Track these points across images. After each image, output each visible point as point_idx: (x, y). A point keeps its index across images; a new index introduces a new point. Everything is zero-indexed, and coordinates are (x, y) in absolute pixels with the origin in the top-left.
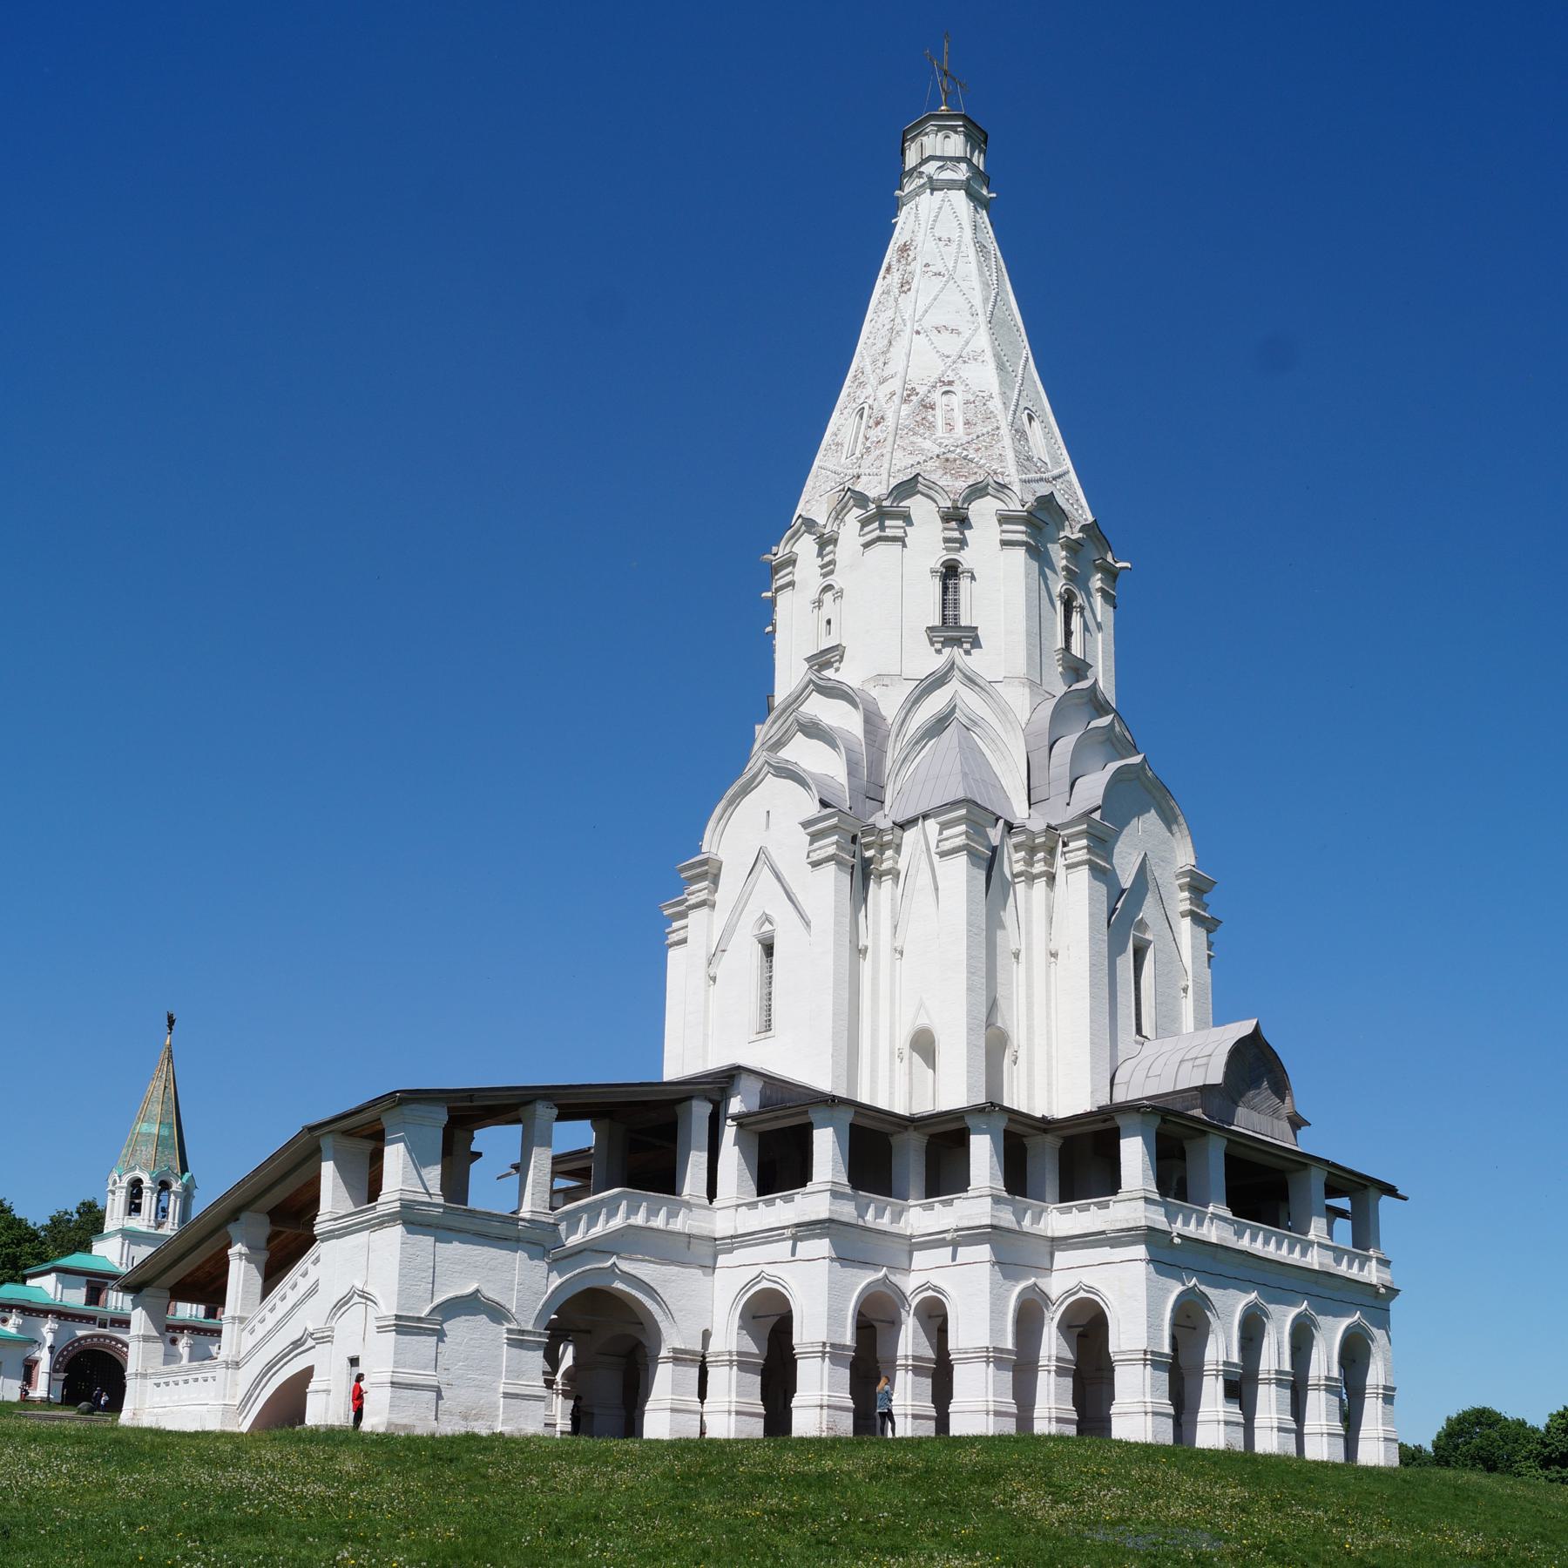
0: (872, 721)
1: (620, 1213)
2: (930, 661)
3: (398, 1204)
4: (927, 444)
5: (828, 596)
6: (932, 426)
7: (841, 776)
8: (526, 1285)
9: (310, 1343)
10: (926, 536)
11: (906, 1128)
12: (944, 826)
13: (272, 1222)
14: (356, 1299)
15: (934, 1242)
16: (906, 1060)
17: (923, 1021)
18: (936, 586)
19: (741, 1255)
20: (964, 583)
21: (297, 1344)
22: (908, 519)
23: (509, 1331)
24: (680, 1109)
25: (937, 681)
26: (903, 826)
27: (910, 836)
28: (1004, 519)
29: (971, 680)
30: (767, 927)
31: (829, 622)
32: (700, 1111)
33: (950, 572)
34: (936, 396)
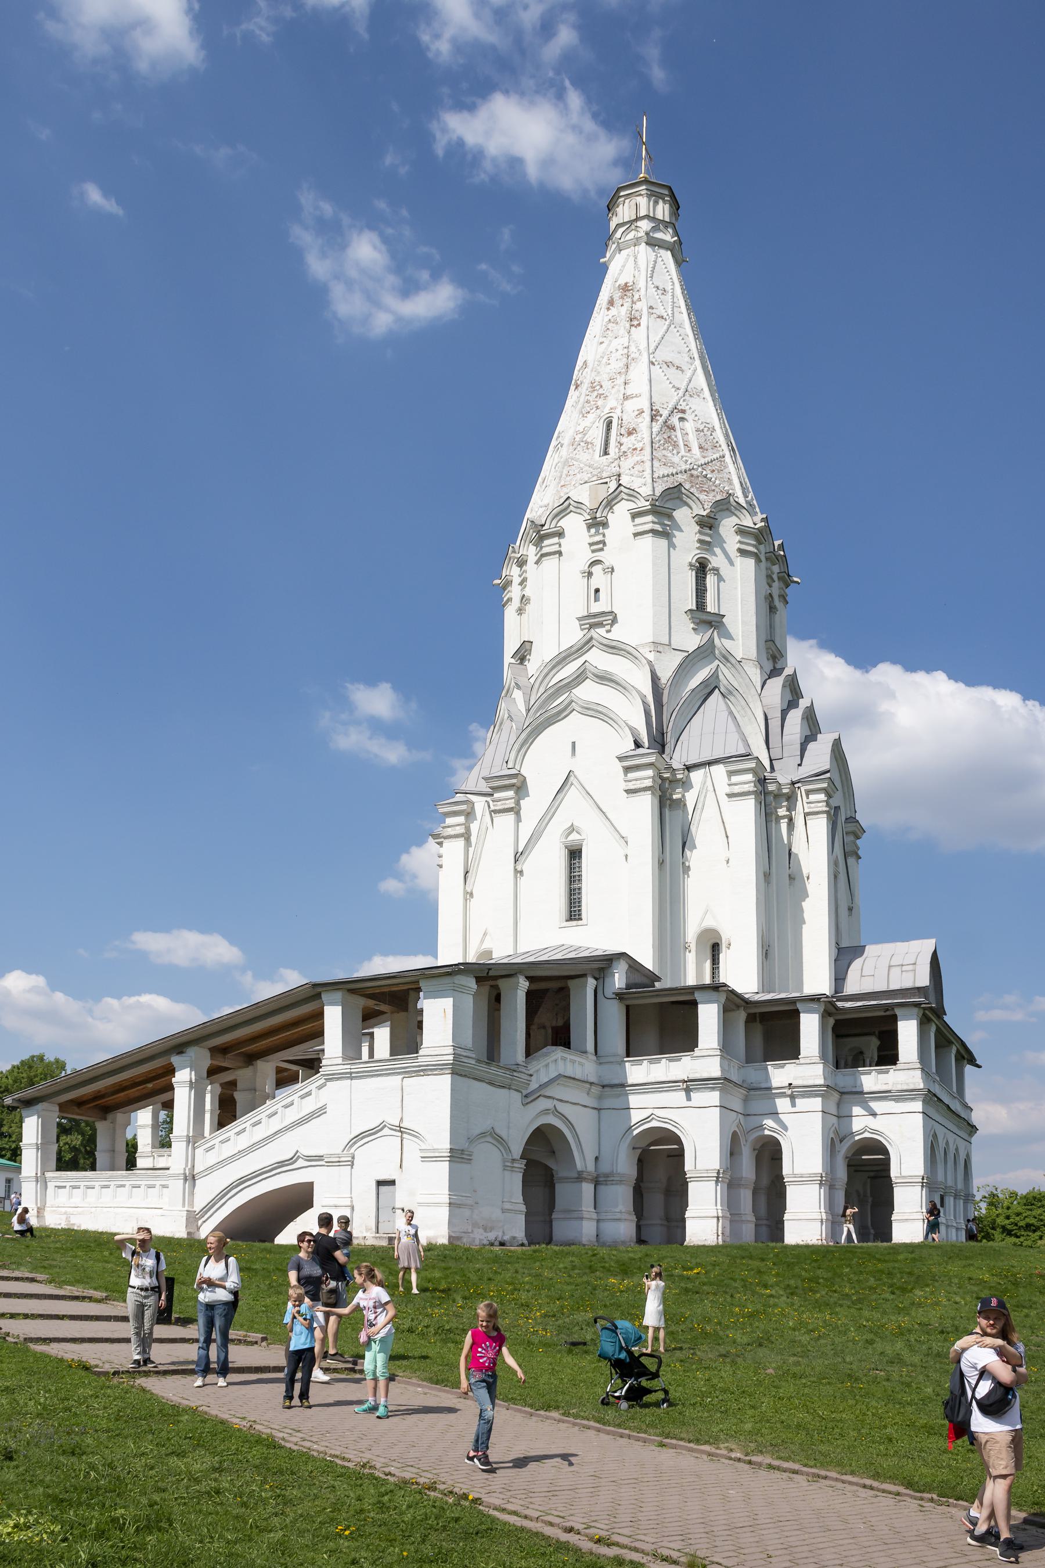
0: (655, 679)
2: (691, 640)
4: (676, 459)
5: (597, 570)
6: (675, 445)
9: (301, 1163)
12: (731, 773)
13: (212, 1057)
17: (709, 923)
18: (691, 577)
20: (710, 580)
21: (282, 1164)
26: (689, 768)
27: (696, 776)
28: (741, 531)
29: (726, 657)
30: (574, 836)
31: (597, 591)
32: (591, 983)
33: (701, 569)
34: (674, 420)
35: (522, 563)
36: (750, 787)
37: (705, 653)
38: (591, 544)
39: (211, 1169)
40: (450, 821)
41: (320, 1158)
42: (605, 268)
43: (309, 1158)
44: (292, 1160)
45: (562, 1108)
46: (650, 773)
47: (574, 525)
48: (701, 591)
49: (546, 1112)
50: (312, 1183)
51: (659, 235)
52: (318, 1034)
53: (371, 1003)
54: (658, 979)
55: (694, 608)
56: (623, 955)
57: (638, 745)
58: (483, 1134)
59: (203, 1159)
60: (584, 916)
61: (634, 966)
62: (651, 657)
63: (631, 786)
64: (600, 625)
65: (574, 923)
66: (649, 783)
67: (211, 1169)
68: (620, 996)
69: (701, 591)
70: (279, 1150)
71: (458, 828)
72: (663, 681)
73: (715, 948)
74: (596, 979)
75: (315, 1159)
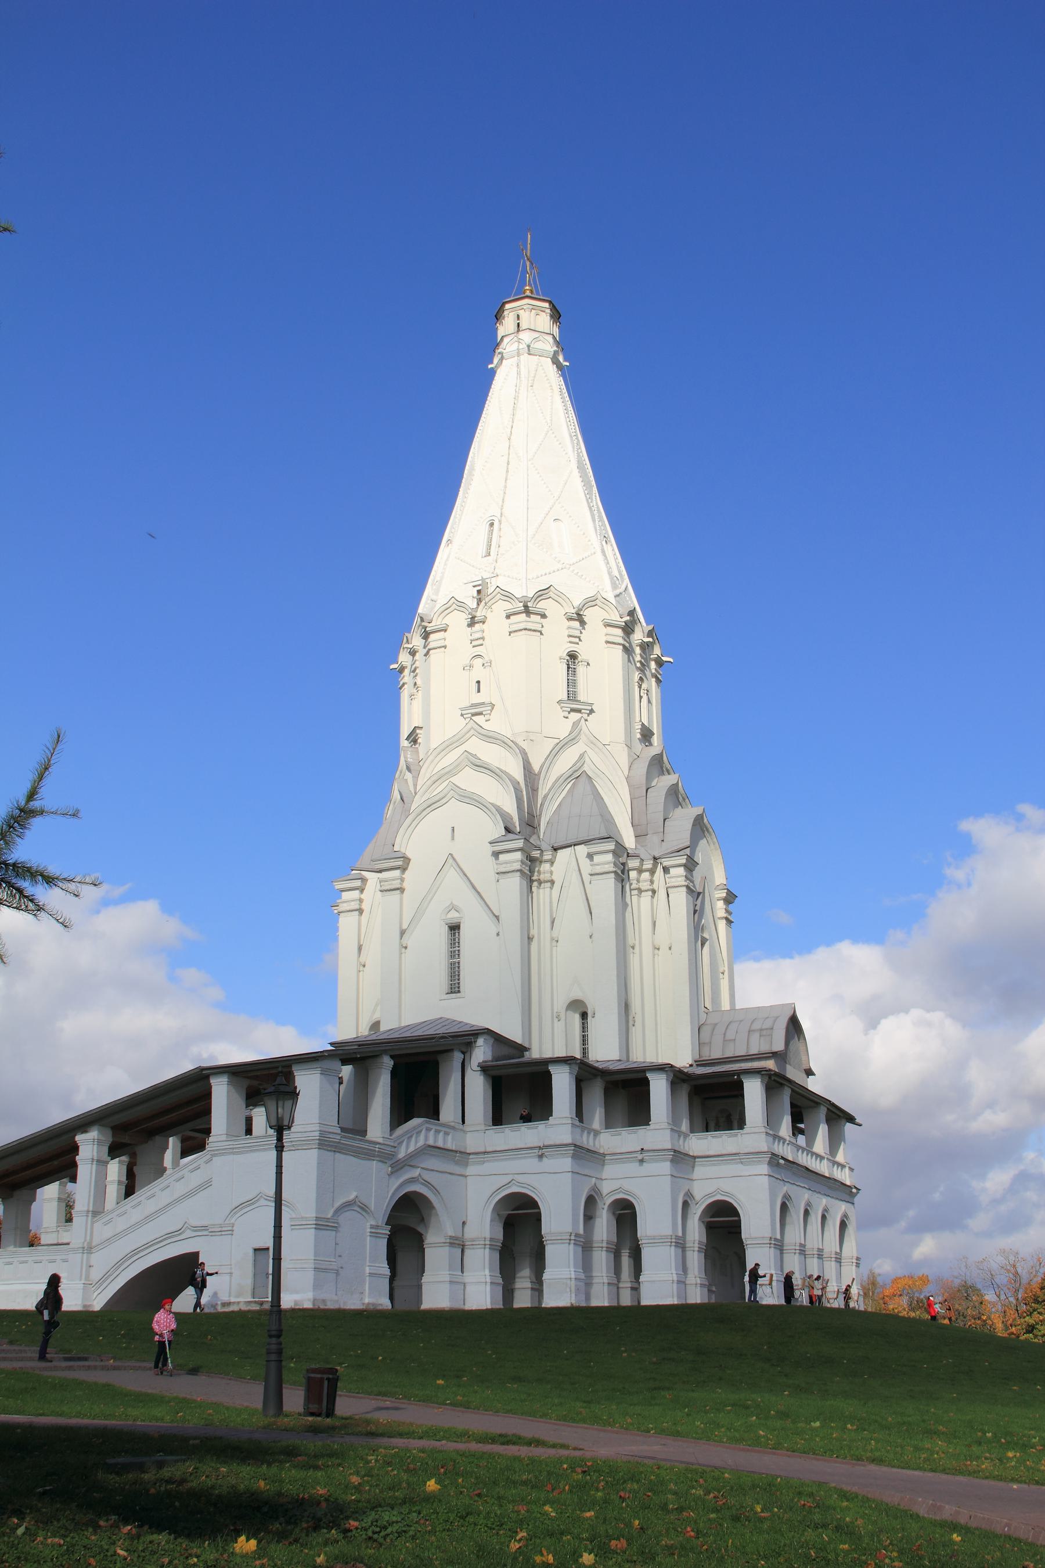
1: (418, 1132)
2: (562, 727)
3: (317, 1134)
5: (478, 662)
7: (510, 807)
8: (380, 1190)
9: (189, 1233)
10: (557, 632)
11: (595, 1076)
13: (113, 1136)
14: (262, 1202)
15: (621, 1157)
16: (563, 1022)
17: (577, 994)
19: (491, 1166)
20: (581, 669)
21: (171, 1235)
22: (544, 616)
23: (372, 1227)
24: (440, 1058)
25: (571, 740)
29: (594, 741)
32: (458, 1056)
35: (413, 653)
36: (611, 868)
37: (571, 740)
38: (472, 641)
39: (109, 1241)
40: (346, 896)
41: (205, 1228)
42: (493, 373)
43: (196, 1229)
44: (179, 1231)
45: (427, 1176)
46: (518, 855)
47: (457, 621)
48: (571, 683)
49: (412, 1180)
50: (196, 1255)
51: (539, 345)
52: (207, 1112)
53: (255, 1083)
54: (526, 1049)
55: (565, 697)
56: (488, 1032)
57: (508, 830)
58: (348, 1205)
59: (102, 1231)
60: (461, 989)
61: (498, 1039)
62: (524, 745)
63: (500, 870)
64: (480, 714)
65: (453, 995)
66: (517, 866)
67: (109, 1241)
68: (484, 1069)
69: (571, 683)
70: (168, 1223)
71: (353, 903)
72: (536, 768)
73: (584, 1016)
74: (463, 1053)
75: (202, 1229)
